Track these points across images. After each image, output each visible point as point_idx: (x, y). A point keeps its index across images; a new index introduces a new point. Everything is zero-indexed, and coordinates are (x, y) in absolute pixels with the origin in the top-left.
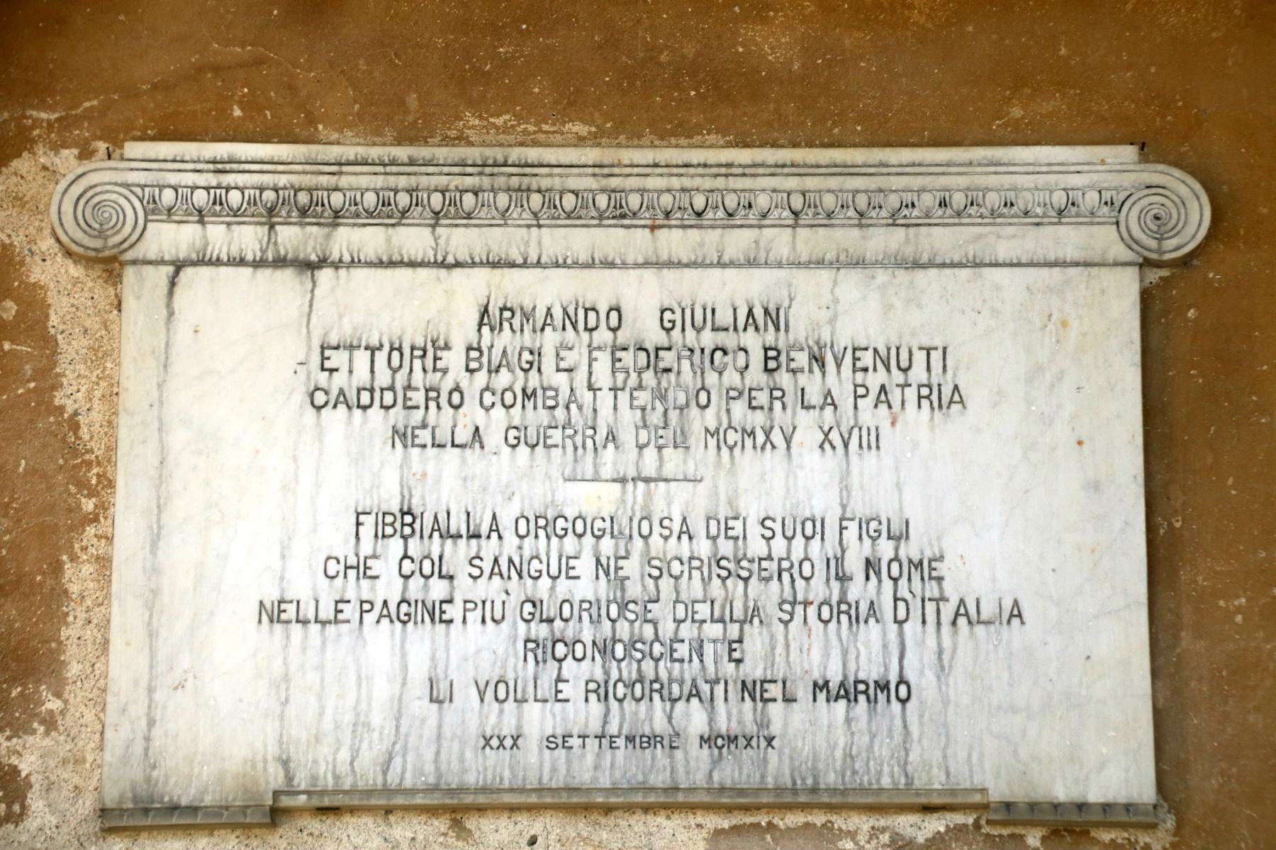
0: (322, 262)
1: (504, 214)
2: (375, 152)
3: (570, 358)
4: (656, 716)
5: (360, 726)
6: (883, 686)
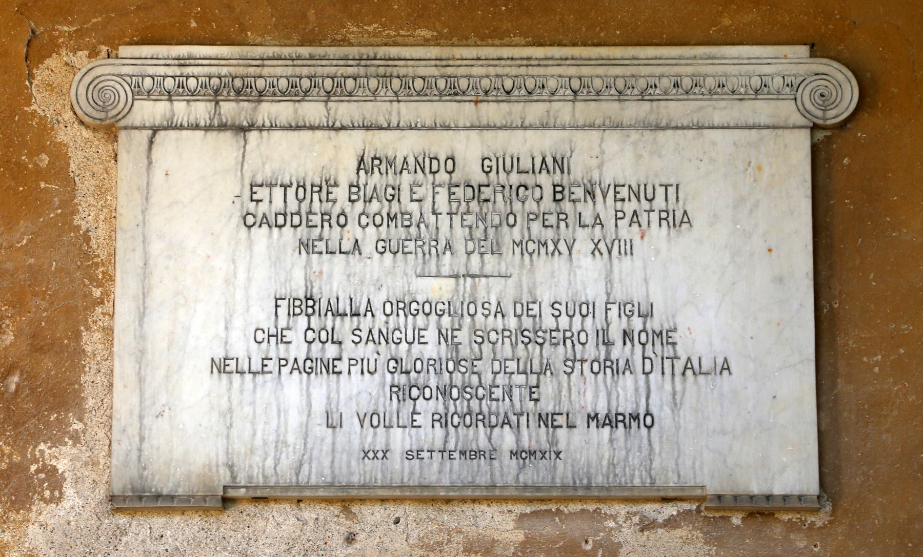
0: (251, 127)
1: (374, 92)
2: (286, 51)
3: (420, 192)
4: (480, 437)
5: (281, 443)
6: (635, 417)
